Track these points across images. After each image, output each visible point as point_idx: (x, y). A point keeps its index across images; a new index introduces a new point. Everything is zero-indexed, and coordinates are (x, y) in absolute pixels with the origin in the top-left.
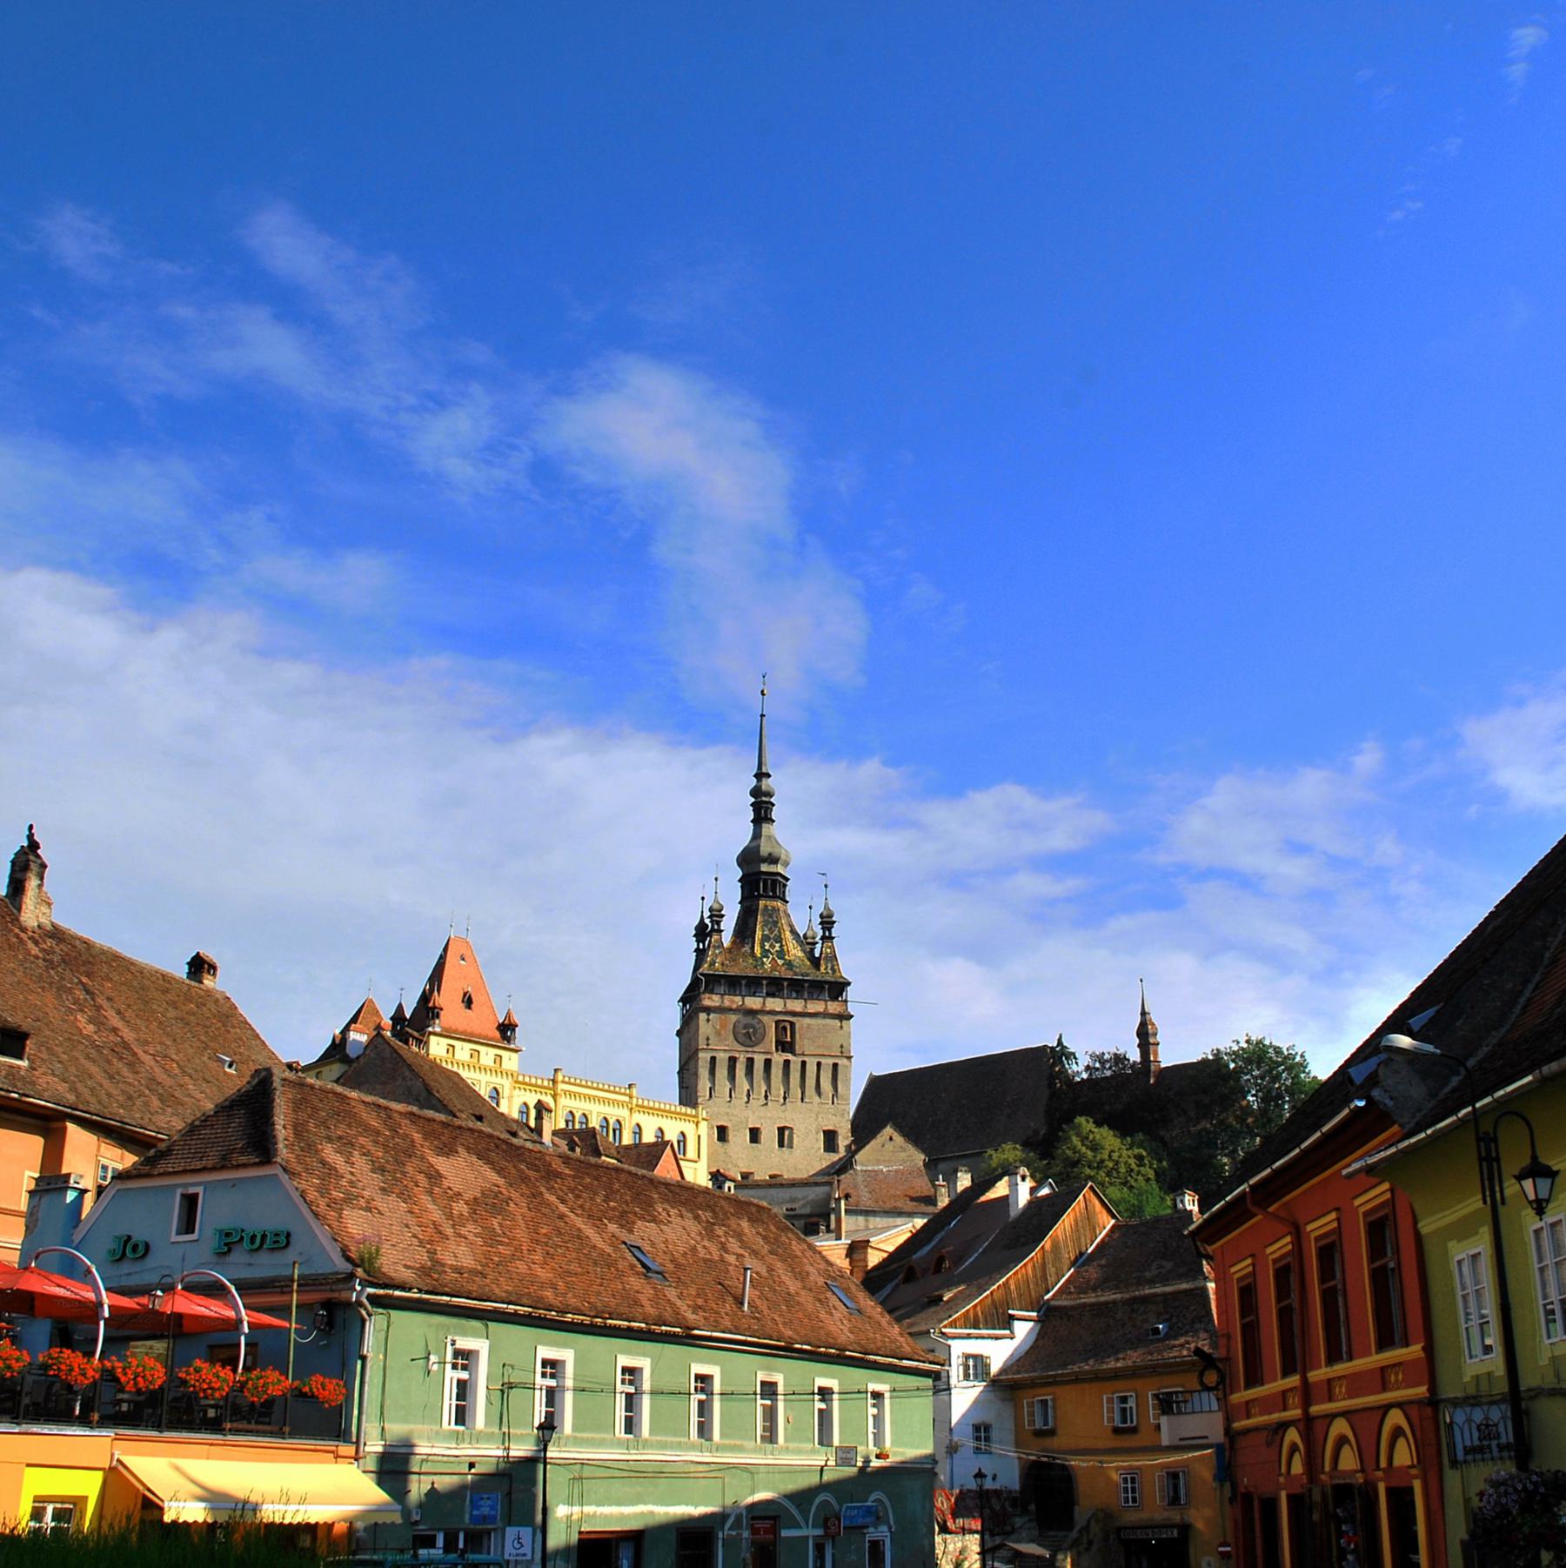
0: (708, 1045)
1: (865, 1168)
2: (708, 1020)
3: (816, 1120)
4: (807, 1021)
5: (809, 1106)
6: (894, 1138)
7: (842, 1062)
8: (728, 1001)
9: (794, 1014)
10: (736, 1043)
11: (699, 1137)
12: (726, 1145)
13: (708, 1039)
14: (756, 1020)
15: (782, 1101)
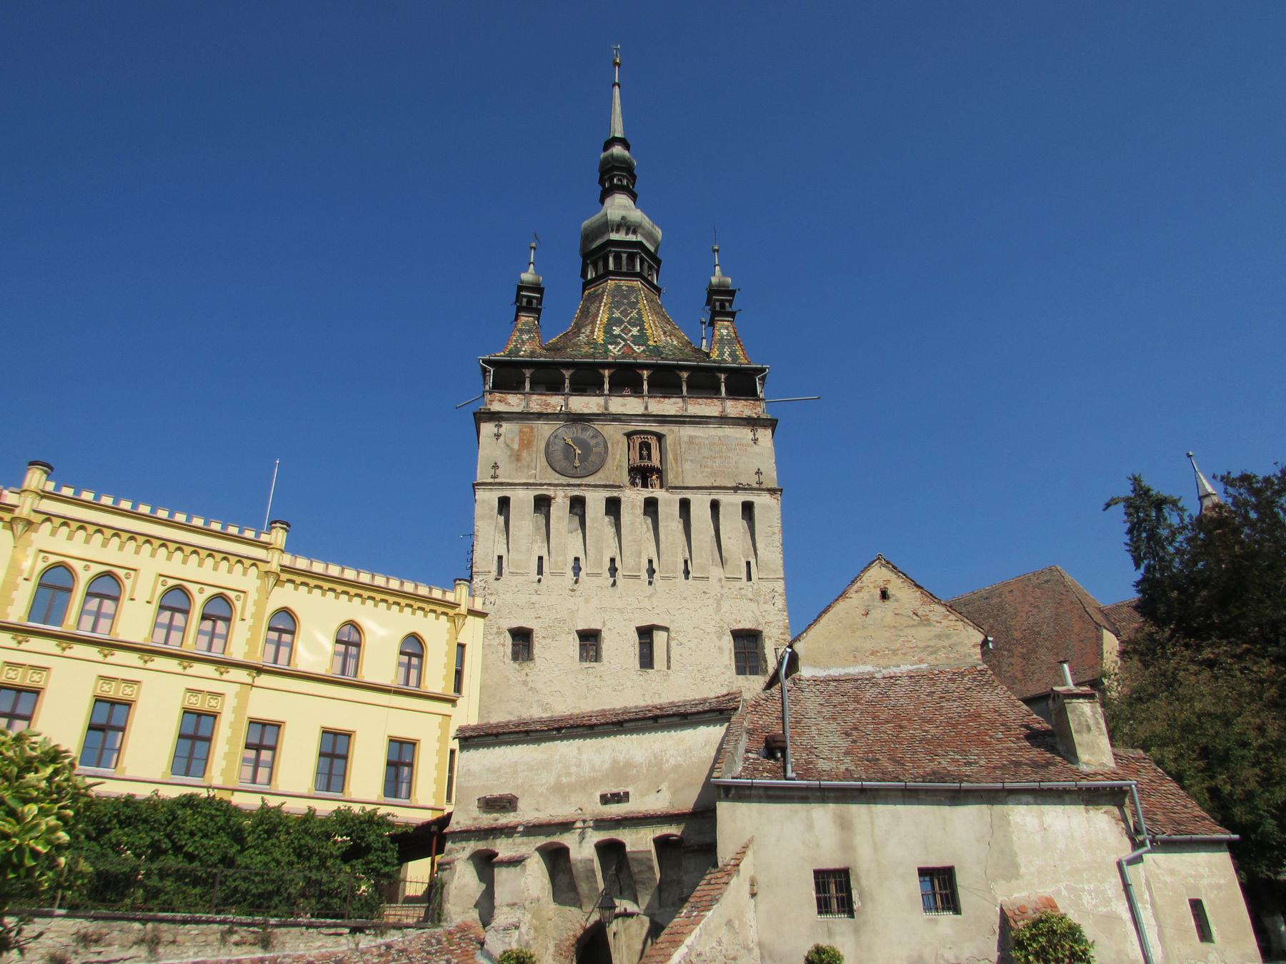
0: (494, 477)
1: (821, 673)
2: (498, 436)
3: (718, 609)
4: (687, 431)
5: (701, 585)
6: (889, 592)
7: (762, 501)
8: (536, 403)
9: (663, 419)
10: (549, 467)
11: (461, 646)
12: (527, 667)
13: (495, 466)
14: (590, 433)
15: (645, 576)
